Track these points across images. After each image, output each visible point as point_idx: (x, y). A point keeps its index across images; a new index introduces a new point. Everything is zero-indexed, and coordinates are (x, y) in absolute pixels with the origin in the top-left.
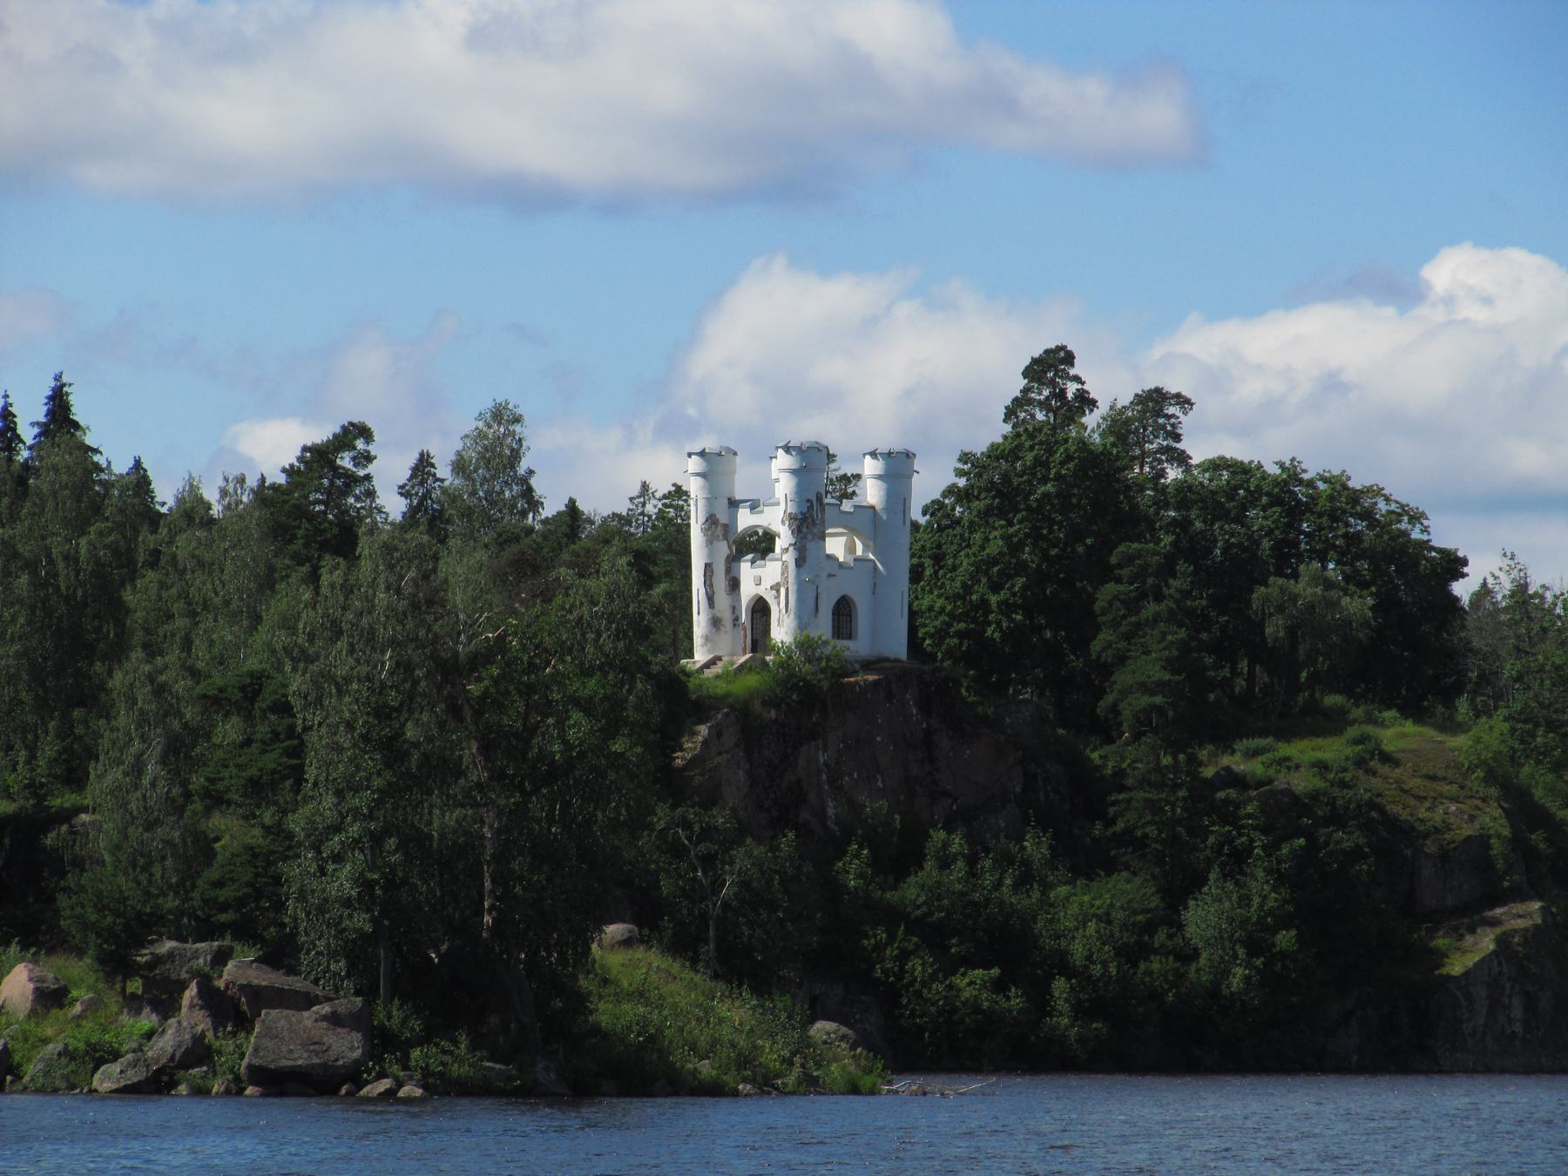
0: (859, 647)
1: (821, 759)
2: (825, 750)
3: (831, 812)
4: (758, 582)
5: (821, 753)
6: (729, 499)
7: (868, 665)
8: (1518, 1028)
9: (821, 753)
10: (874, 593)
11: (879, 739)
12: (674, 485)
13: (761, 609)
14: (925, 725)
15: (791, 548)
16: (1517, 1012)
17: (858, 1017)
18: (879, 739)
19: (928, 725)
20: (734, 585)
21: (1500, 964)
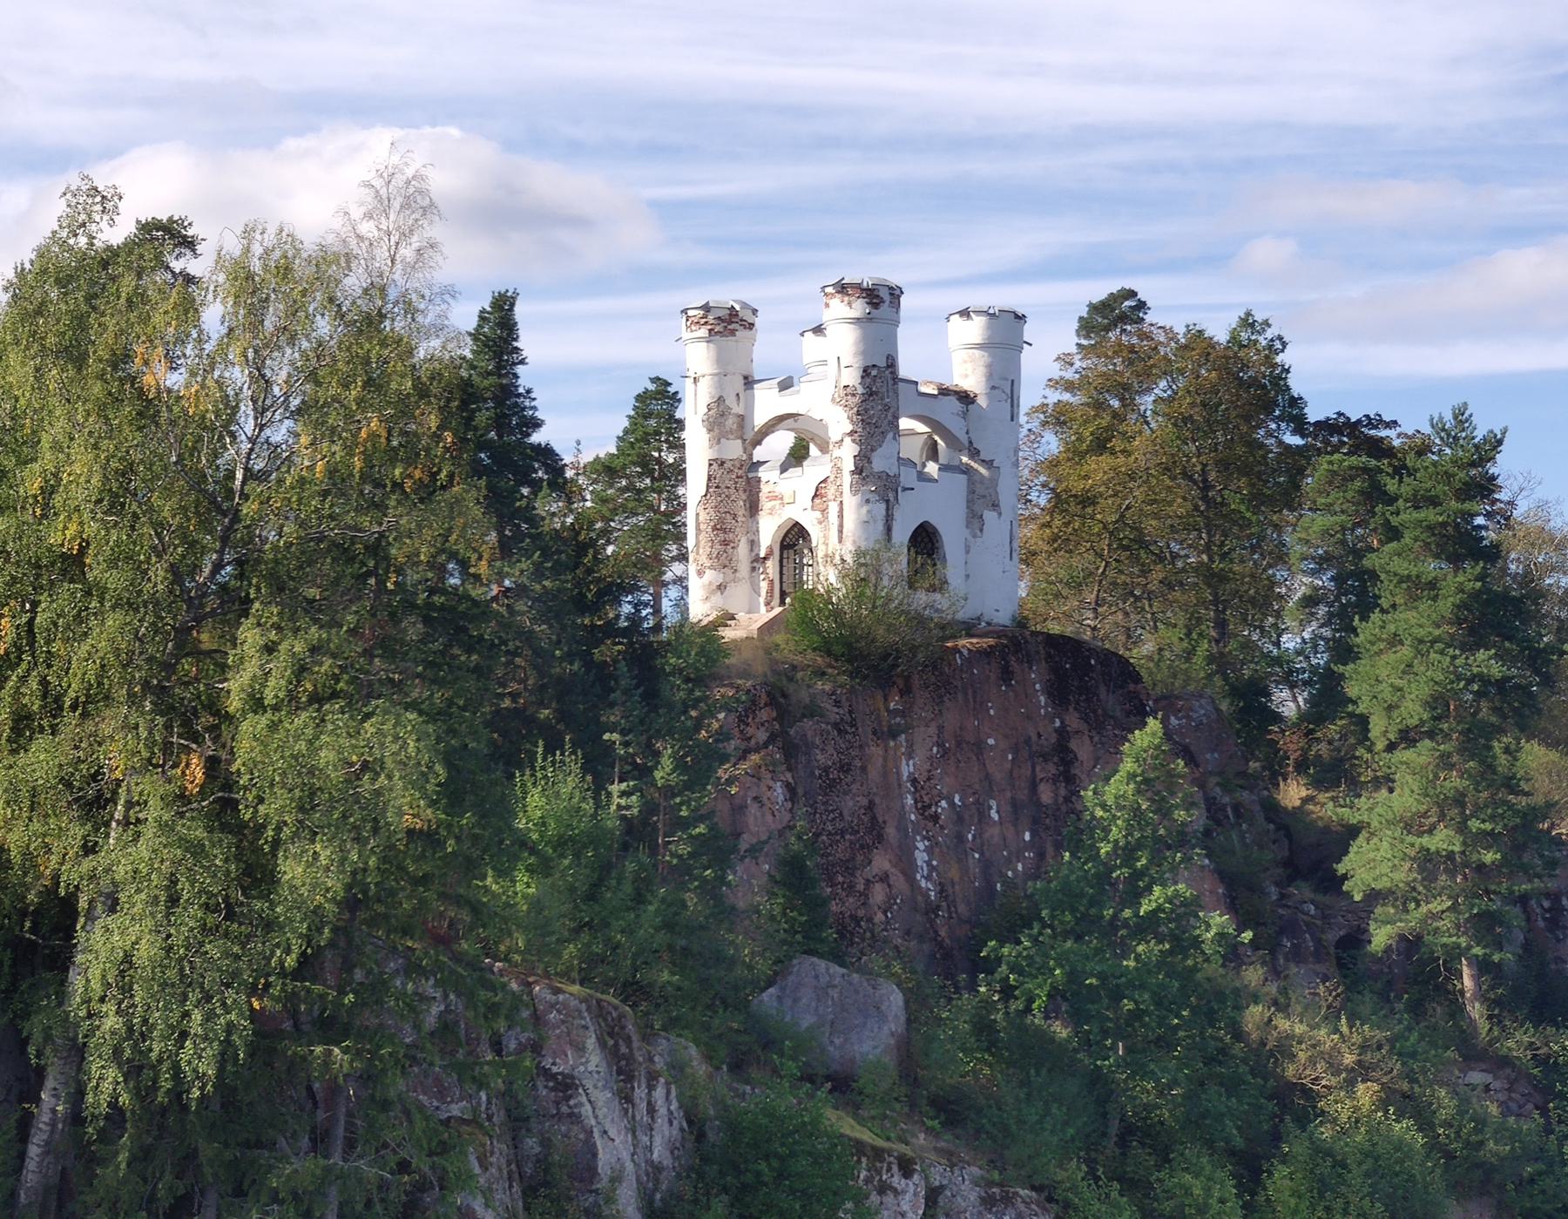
1: (906, 769)
2: (910, 756)
3: (921, 857)
5: (904, 762)
6: (746, 378)
7: (969, 628)
9: (904, 762)
11: (991, 741)
13: (794, 539)
14: (1058, 723)
15: (848, 440)
18: (991, 741)
19: (1062, 722)
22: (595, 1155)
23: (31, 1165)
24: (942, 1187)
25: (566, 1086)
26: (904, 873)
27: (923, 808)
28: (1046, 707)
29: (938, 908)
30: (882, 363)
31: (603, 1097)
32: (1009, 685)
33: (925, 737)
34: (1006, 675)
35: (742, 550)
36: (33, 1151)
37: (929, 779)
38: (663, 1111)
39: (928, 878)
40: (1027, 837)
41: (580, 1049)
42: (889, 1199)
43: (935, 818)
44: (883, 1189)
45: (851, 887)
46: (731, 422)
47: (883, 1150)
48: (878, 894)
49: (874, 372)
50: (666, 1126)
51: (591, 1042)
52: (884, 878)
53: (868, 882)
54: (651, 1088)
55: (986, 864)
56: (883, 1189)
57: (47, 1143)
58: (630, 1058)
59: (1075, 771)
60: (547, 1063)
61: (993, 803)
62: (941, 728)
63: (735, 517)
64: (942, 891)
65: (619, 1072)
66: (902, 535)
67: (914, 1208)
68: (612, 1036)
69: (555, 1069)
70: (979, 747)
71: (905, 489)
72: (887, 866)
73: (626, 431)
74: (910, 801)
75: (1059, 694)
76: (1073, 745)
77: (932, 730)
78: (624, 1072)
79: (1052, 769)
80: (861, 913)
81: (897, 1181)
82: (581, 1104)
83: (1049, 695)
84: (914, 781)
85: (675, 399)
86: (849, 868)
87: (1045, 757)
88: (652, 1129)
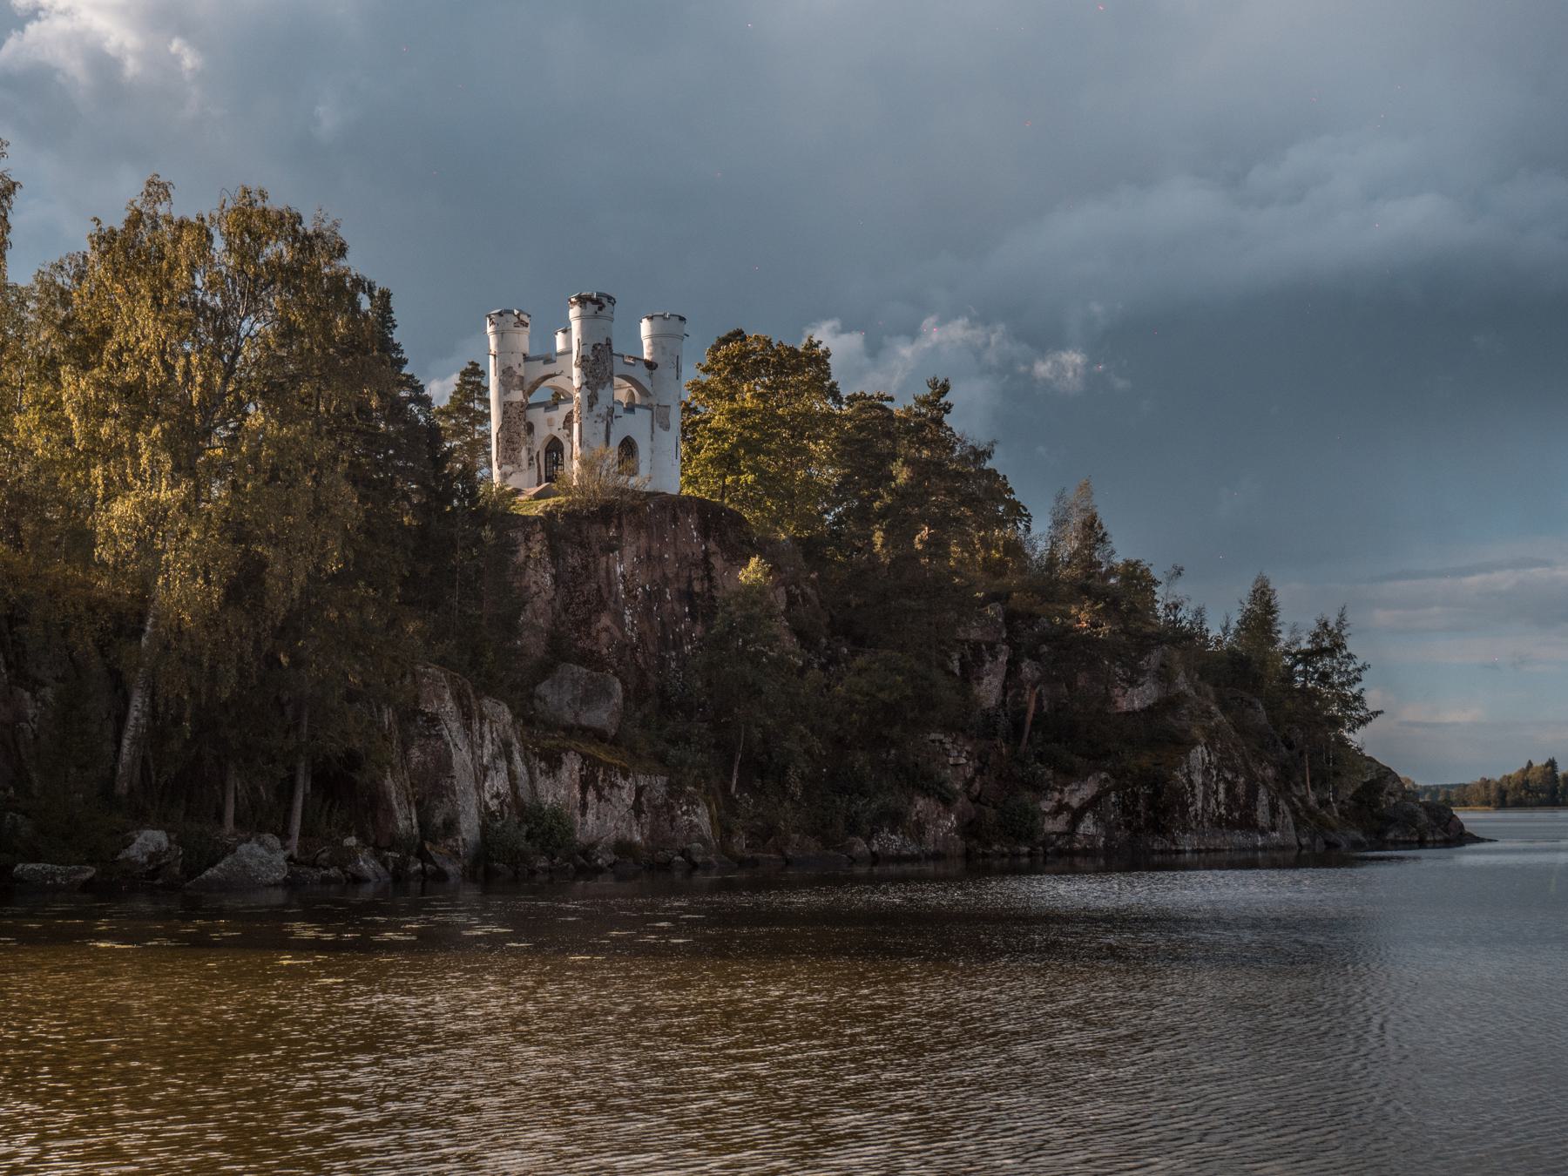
0: (641, 481)
2: (621, 562)
3: (628, 619)
4: (550, 423)
8: (1223, 812)
10: (652, 439)
11: (666, 556)
12: (472, 363)
13: (555, 448)
14: (704, 548)
15: (584, 387)
16: (1222, 796)
17: (685, 808)
20: (530, 428)
21: (1209, 755)
22: (451, 757)
23: (125, 750)
24: (644, 786)
25: (434, 720)
26: (619, 628)
27: (628, 592)
28: (697, 538)
29: (638, 647)
30: (604, 343)
31: (455, 726)
32: (676, 525)
33: (630, 551)
34: (675, 519)
35: (524, 454)
36: (126, 742)
37: (632, 575)
38: (488, 737)
39: (632, 630)
40: (687, 609)
41: (441, 699)
42: (616, 790)
43: (636, 597)
44: (612, 785)
45: (589, 635)
46: (516, 381)
47: (612, 764)
48: (604, 636)
49: (599, 348)
50: (490, 746)
51: (447, 696)
52: (607, 629)
53: (598, 631)
54: (481, 724)
55: (663, 624)
56: (612, 785)
57: (134, 738)
58: (470, 707)
59: (713, 575)
60: (422, 707)
61: (668, 590)
62: (638, 548)
63: (519, 434)
64: (640, 636)
65: (464, 714)
66: (615, 442)
67: (629, 796)
68: (459, 697)
69: (427, 710)
70: (661, 557)
71: (616, 417)
72: (609, 623)
73: (455, 393)
74: (621, 587)
75: (705, 532)
76: (712, 560)
77: (634, 548)
78: (467, 716)
79: (701, 573)
80: (595, 648)
81: (620, 781)
82: (443, 729)
83: (699, 532)
84: (624, 576)
85: (483, 374)
86: (587, 622)
87: (696, 565)
88: (482, 747)
